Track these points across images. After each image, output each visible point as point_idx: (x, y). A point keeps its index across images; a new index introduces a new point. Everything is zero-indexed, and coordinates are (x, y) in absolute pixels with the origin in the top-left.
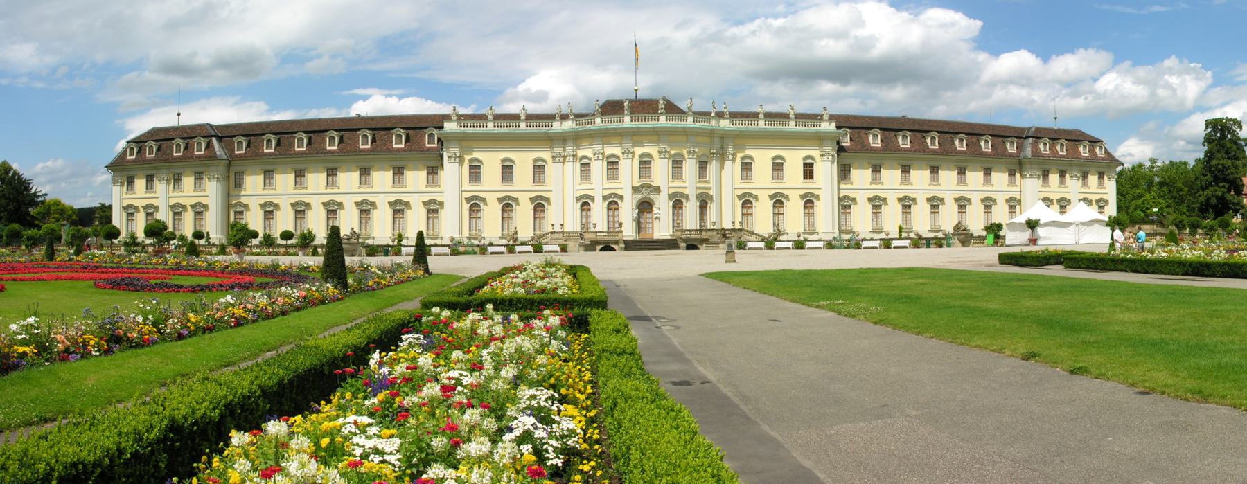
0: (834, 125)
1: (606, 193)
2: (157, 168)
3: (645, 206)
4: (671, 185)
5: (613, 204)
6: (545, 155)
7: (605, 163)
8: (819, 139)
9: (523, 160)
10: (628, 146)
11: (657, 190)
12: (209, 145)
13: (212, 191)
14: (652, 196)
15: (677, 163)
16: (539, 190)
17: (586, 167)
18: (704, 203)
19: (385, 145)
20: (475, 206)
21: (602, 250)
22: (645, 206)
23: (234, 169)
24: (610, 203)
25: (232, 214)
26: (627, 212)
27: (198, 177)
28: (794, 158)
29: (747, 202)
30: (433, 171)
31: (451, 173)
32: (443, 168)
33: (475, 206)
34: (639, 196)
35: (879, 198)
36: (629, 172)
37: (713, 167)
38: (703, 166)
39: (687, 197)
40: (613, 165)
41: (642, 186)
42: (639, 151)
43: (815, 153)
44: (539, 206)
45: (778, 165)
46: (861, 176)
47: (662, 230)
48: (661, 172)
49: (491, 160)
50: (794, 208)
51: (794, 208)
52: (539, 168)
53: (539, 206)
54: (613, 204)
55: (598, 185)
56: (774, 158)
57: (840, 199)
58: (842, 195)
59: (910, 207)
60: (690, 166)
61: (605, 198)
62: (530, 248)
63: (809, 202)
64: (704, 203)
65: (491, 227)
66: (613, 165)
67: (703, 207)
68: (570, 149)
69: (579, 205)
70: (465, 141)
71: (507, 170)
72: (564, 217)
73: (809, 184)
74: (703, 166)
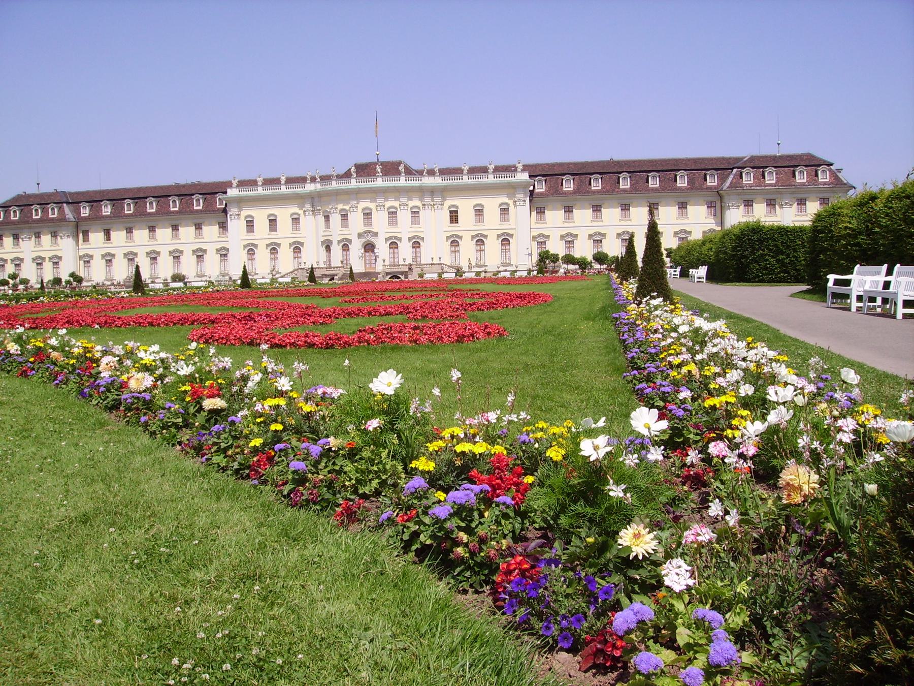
1: (411, 235)
2: (59, 226)
4: (411, 230)
9: (284, 214)
16: (297, 237)
17: (327, 218)
19: (189, 207)
27: (54, 235)
30: (223, 226)
31: (236, 225)
38: (415, 213)
39: (400, 239)
49: (260, 215)
52: (296, 220)
60: (404, 216)
61: (339, 242)
67: (416, 245)
70: (240, 202)
74: (415, 213)
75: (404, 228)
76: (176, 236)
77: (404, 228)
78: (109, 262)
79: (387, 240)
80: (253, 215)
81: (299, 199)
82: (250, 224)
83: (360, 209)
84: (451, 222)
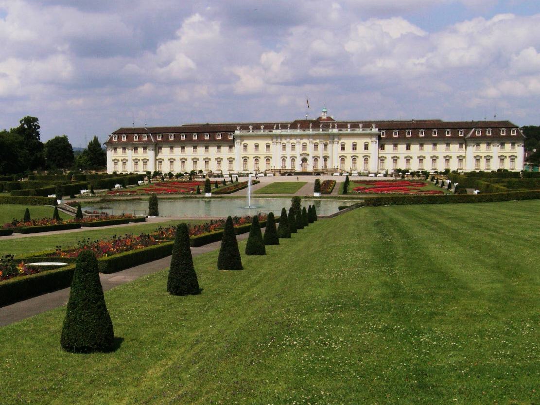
0: (377, 129)
3: (304, 160)
5: (293, 159)
6: (270, 142)
7: (291, 146)
8: (371, 135)
9: (262, 143)
10: (298, 140)
11: (308, 155)
12: (148, 137)
13: (150, 153)
14: (307, 157)
15: (316, 146)
16: (268, 154)
17: (284, 146)
18: (326, 159)
20: (245, 160)
21: (288, 175)
22: (304, 160)
23: (158, 146)
24: (284, 159)
25: (157, 162)
26: (298, 161)
28: (360, 142)
29: (343, 159)
31: (238, 147)
32: (234, 147)
33: (245, 160)
34: (302, 157)
35: (396, 157)
36: (299, 149)
37: (329, 146)
38: (326, 146)
39: (319, 157)
40: (293, 146)
41: (303, 154)
42: (303, 141)
43: (368, 140)
44: (268, 159)
45: (257, 147)
46: (389, 148)
47: (310, 169)
48: (310, 149)
49: (251, 143)
50: (360, 161)
51: (360, 161)
52: (268, 147)
53: (268, 159)
54: (293, 159)
55: (289, 153)
56: (353, 143)
57: (379, 158)
58: (379, 156)
59: (409, 160)
60: (321, 147)
61: (290, 157)
62: (263, 175)
63: (366, 159)
64: (326, 159)
65: (251, 167)
66: (293, 146)
68: (279, 140)
69: (282, 160)
70: (242, 137)
71: (257, 147)
72: (277, 164)
73: (366, 152)
74: (326, 146)
75: (321, 152)
76: (447, 149)
77: (321, 152)
78: (231, 162)
79: (313, 157)
80: (247, 143)
81: (272, 137)
82: (245, 147)
83: (301, 143)
84: (342, 150)
